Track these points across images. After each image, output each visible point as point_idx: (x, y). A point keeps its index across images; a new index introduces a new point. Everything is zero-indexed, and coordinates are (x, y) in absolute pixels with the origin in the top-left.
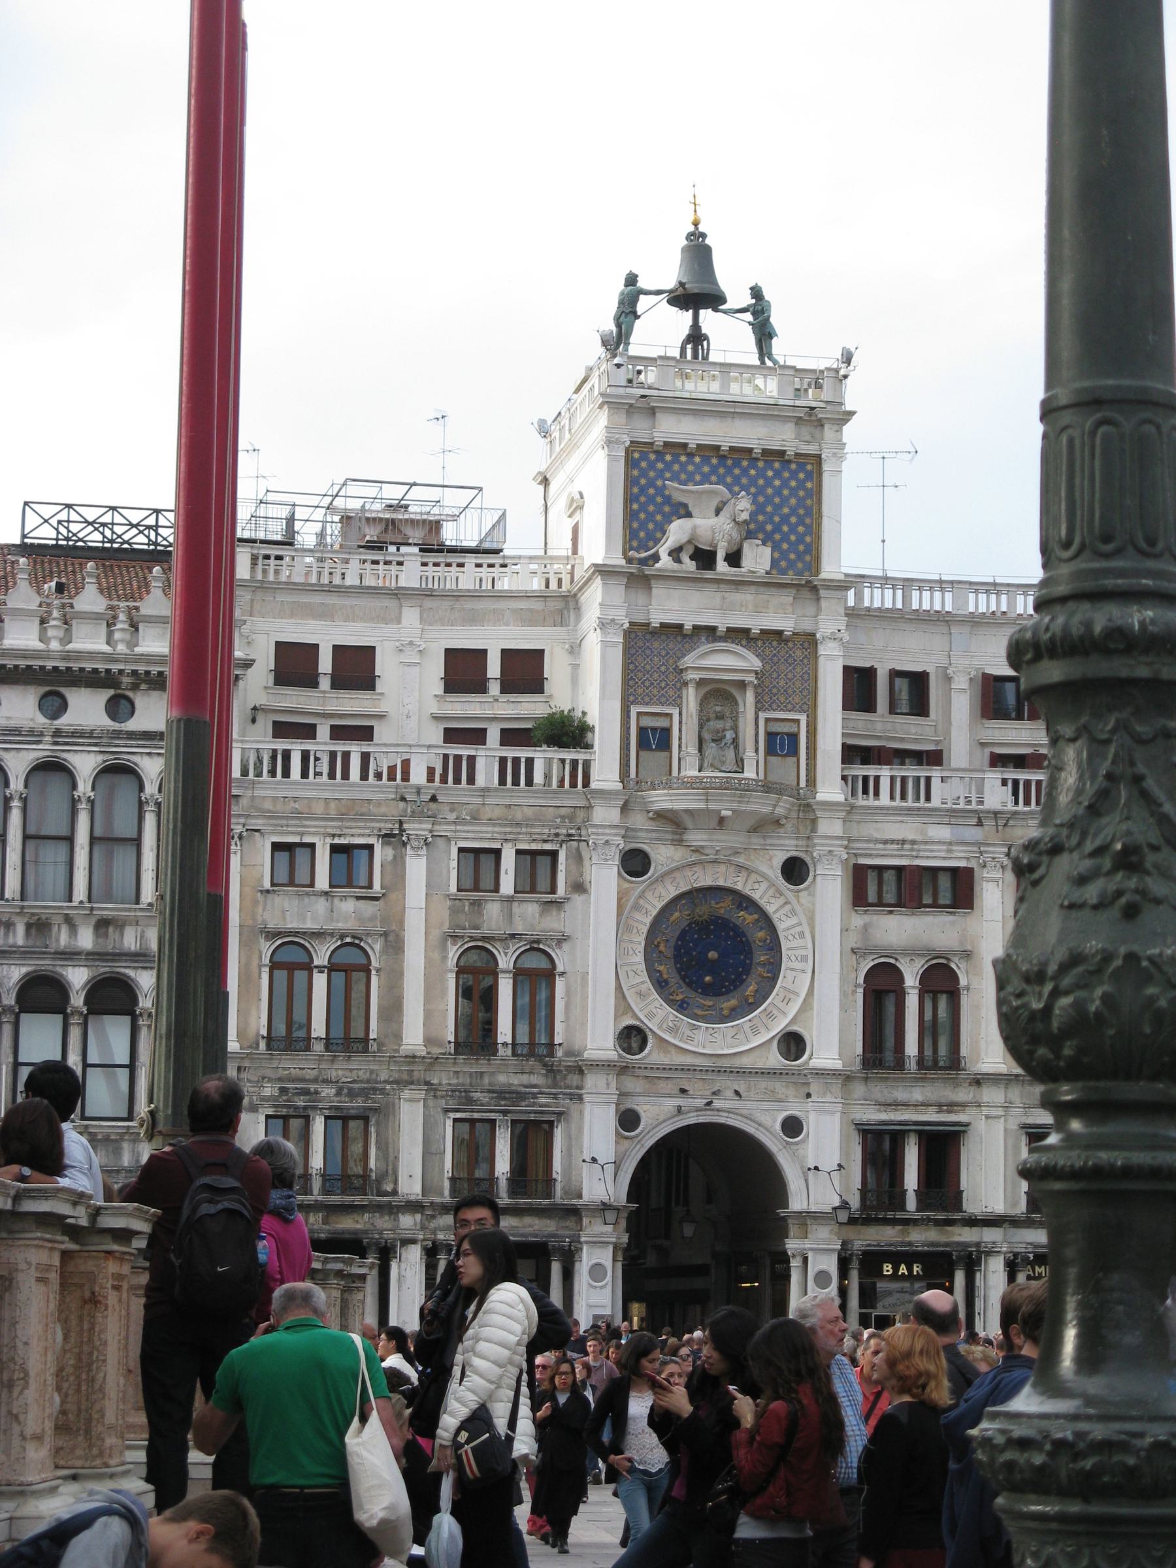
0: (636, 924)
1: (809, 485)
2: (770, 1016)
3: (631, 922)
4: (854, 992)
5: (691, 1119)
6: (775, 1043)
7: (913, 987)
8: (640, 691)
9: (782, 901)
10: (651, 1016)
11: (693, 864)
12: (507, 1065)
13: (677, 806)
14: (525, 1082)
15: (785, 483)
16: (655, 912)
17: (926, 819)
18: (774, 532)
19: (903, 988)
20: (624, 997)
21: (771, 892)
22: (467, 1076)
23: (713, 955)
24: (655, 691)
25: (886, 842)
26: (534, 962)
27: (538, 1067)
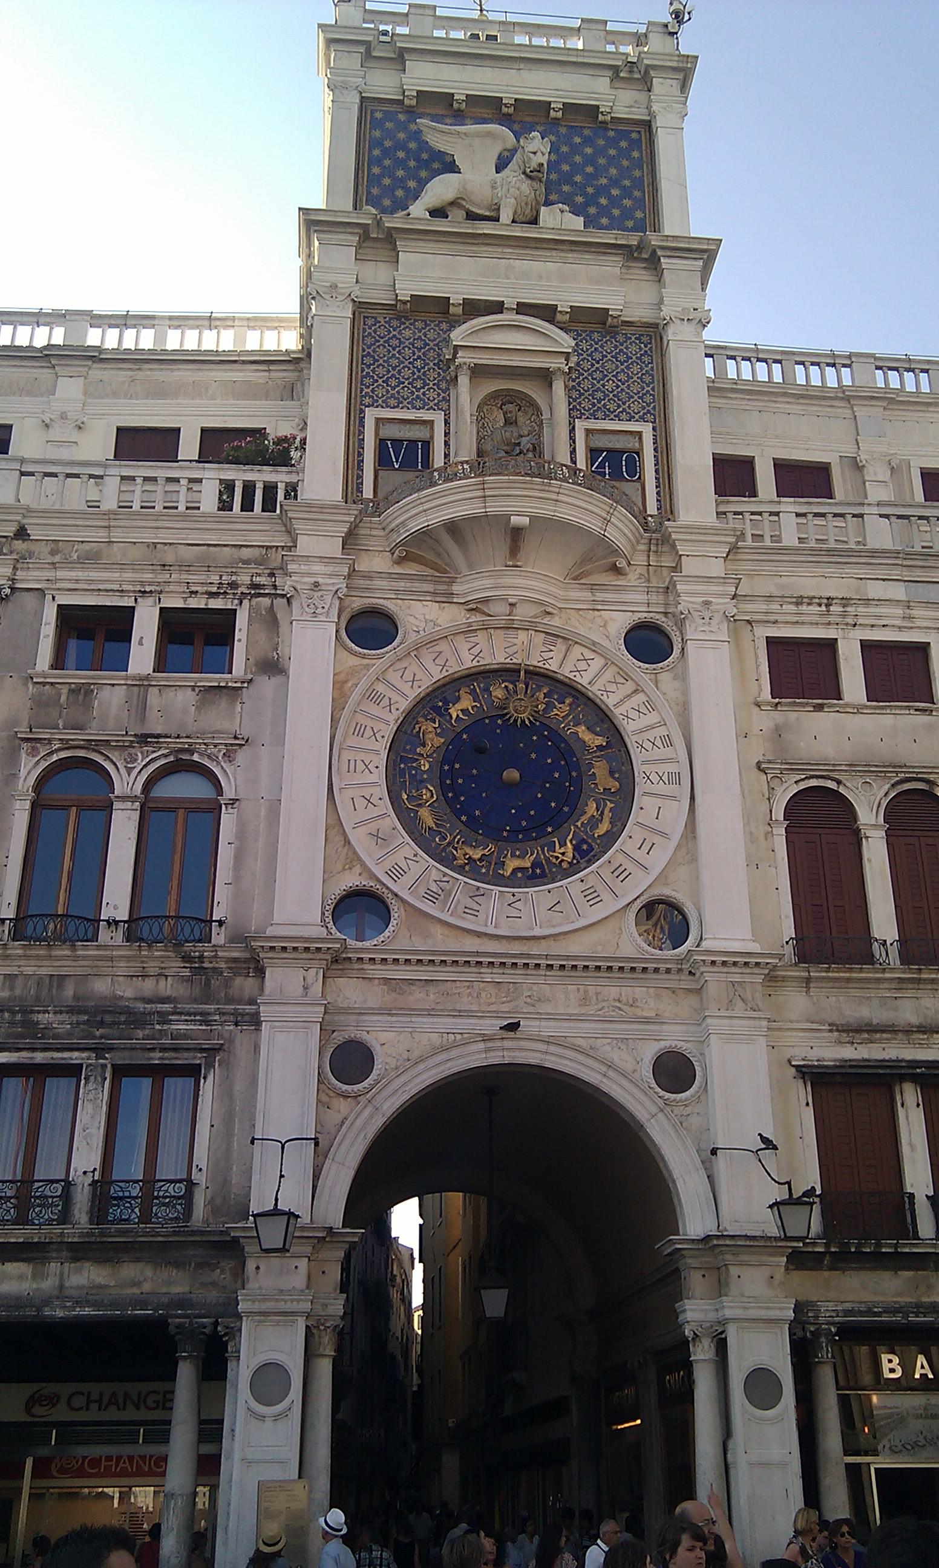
0: (370, 723)
1: (636, 154)
2: (620, 873)
3: (361, 719)
4: (769, 835)
5: (475, 1057)
6: (632, 916)
7: (875, 826)
8: (380, 392)
9: (630, 686)
10: (396, 872)
11: (468, 631)
12: (111, 959)
13: (436, 518)
14: (147, 994)
15: (601, 152)
16: (404, 705)
17: (862, 572)
18: (587, 204)
19: (857, 832)
20: (347, 842)
21: (609, 674)
22: (32, 983)
23: (512, 774)
24: (406, 393)
25: (799, 601)
26: (184, 788)
27: (175, 966)
